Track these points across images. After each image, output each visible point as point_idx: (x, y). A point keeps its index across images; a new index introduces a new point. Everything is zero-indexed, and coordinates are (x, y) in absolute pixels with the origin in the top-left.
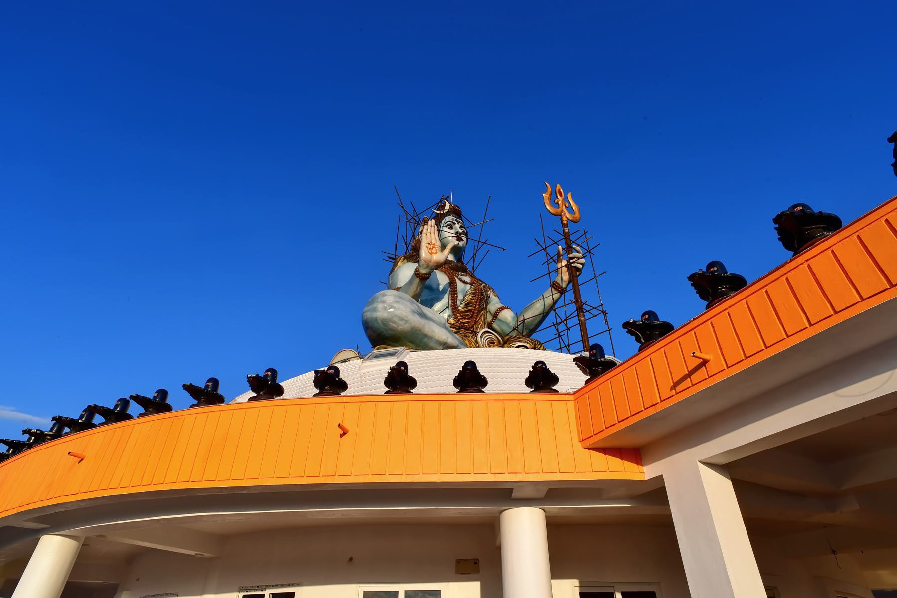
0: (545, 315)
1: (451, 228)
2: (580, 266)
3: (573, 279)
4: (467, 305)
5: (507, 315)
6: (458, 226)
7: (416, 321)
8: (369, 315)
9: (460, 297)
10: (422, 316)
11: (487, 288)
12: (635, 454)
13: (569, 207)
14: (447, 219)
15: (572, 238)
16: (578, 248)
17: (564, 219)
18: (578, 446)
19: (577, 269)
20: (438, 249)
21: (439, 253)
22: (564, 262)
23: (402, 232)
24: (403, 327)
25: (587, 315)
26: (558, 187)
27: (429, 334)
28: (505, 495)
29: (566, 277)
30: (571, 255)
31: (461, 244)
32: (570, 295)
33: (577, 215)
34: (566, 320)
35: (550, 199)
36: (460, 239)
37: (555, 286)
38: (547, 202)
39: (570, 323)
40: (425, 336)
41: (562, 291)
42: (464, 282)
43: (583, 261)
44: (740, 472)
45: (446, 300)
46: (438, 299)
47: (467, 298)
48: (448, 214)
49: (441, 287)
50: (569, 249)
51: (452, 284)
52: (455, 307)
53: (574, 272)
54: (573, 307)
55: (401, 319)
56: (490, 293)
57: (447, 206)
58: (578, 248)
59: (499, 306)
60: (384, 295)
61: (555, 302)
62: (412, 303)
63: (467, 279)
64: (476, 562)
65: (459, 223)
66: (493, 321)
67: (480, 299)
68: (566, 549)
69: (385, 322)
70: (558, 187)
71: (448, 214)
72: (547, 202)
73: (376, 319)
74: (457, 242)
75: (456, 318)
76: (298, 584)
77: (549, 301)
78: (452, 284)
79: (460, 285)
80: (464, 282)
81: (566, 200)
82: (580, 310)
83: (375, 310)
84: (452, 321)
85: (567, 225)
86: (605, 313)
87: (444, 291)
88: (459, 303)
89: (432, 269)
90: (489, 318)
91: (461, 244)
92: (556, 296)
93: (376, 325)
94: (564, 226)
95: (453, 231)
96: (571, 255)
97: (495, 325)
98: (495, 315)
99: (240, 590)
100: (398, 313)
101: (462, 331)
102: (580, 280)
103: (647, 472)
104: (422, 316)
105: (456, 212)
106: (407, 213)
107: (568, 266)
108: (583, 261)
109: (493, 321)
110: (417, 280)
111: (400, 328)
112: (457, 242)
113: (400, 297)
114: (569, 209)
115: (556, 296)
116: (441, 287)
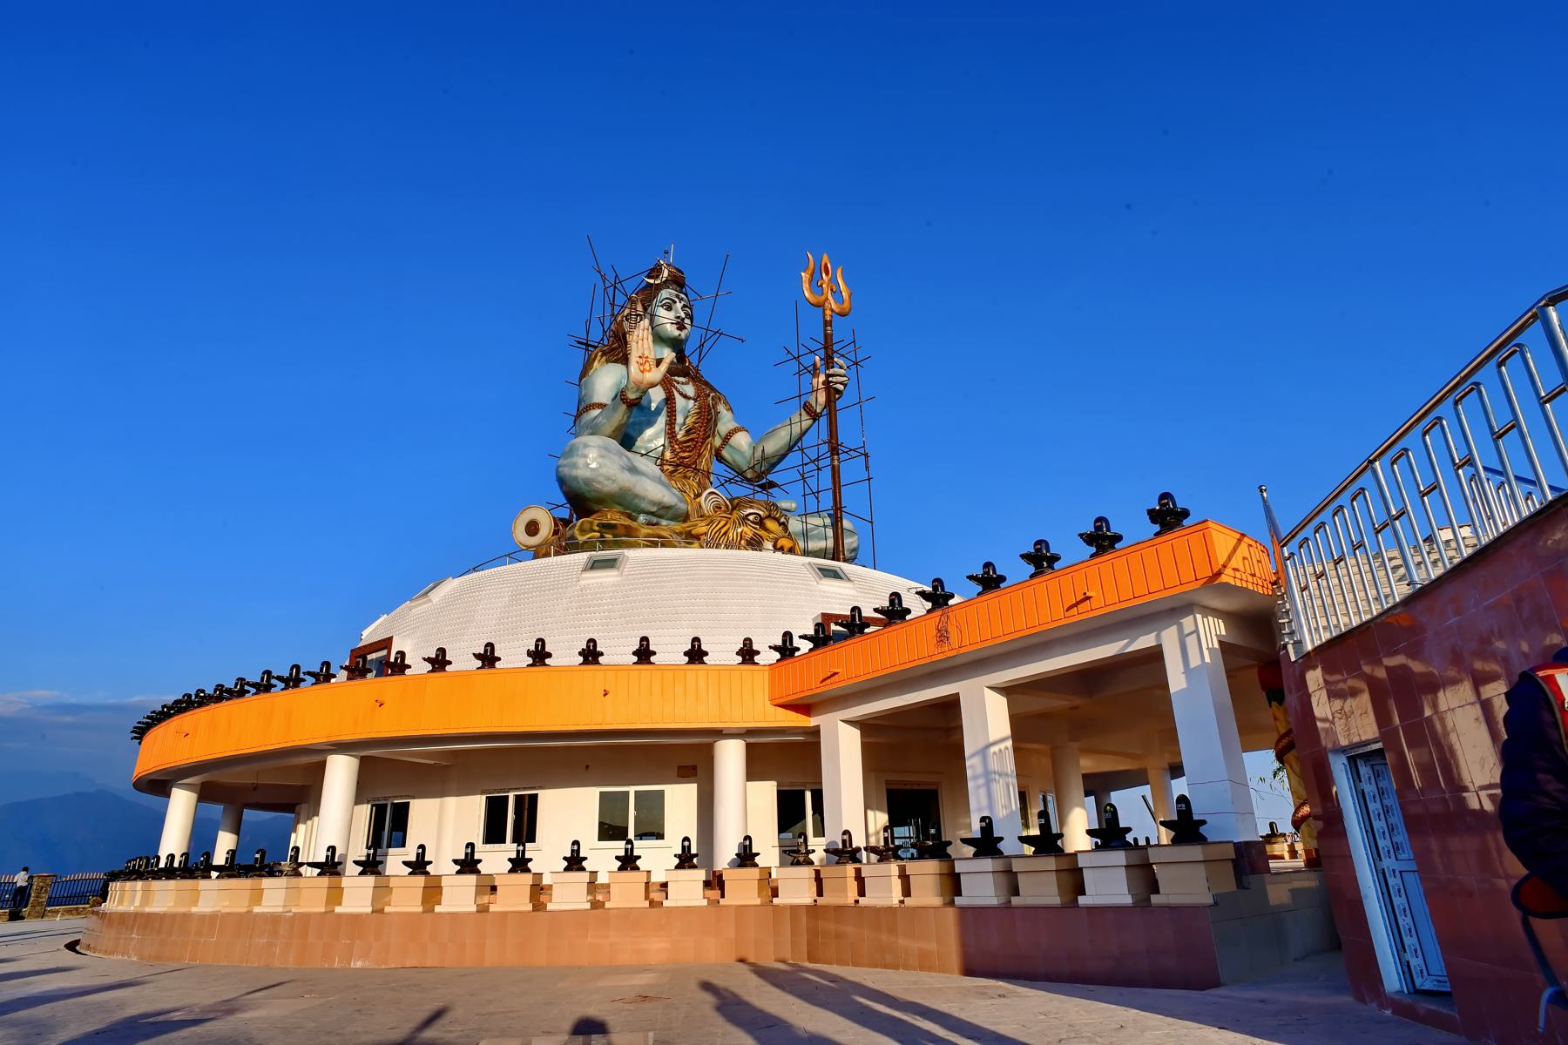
0: (790, 448)
1: (669, 308)
2: (841, 387)
3: (830, 403)
4: (688, 432)
5: (742, 440)
6: (679, 305)
7: (625, 479)
8: (565, 471)
9: (679, 419)
10: (633, 470)
11: (717, 399)
12: (805, 708)
13: (839, 290)
14: (664, 293)
15: (835, 348)
16: (841, 362)
17: (828, 312)
18: (768, 703)
19: (838, 391)
20: (653, 363)
21: (654, 369)
22: (822, 378)
23: (598, 313)
24: (609, 487)
25: (843, 457)
26: (825, 259)
27: (642, 493)
28: (720, 734)
29: (822, 397)
30: (831, 371)
31: (683, 334)
32: (824, 421)
33: (846, 305)
34: (818, 459)
35: (810, 282)
36: (681, 327)
37: (808, 408)
38: (806, 286)
39: (821, 464)
40: (637, 496)
41: (815, 417)
42: (685, 397)
44: (866, 726)
45: (661, 421)
46: (650, 424)
47: (689, 421)
48: (665, 284)
49: (653, 406)
50: (829, 361)
51: (669, 401)
52: (671, 434)
53: (832, 393)
54: (825, 448)
55: (608, 479)
56: (721, 407)
57: (666, 273)
58: (841, 362)
59: (733, 425)
60: (586, 446)
61: (803, 433)
62: (620, 455)
63: (690, 390)
64: (694, 768)
66: (722, 446)
67: (707, 418)
68: (754, 770)
69: (587, 482)
70: (825, 259)
71: (665, 284)
72: (806, 286)
73: (576, 478)
74: (677, 333)
75: (673, 451)
76: (541, 788)
77: (796, 430)
78: (669, 401)
79: (680, 402)
80: (685, 397)
81: (834, 280)
82: (834, 450)
83: (574, 466)
84: (668, 455)
85: (827, 323)
86: (866, 455)
87: (658, 412)
89: (645, 392)
90: (718, 442)
91: (683, 334)
92: (806, 424)
93: (574, 484)
94: (827, 323)
95: (671, 315)
96: (831, 371)
97: (725, 453)
98: (726, 439)
99: (483, 793)
100: (603, 471)
101: (681, 469)
102: (840, 404)
103: (812, 722)
105: (677, 282)
106: (604, 279)
107: (827, 383)
109: (722, 446)
110: (624, 407)
111: (606, 489)
112: (677, 333)
113: (606, 449)
114: (836, 293)
115: (807, 423)
116: (653, 406)
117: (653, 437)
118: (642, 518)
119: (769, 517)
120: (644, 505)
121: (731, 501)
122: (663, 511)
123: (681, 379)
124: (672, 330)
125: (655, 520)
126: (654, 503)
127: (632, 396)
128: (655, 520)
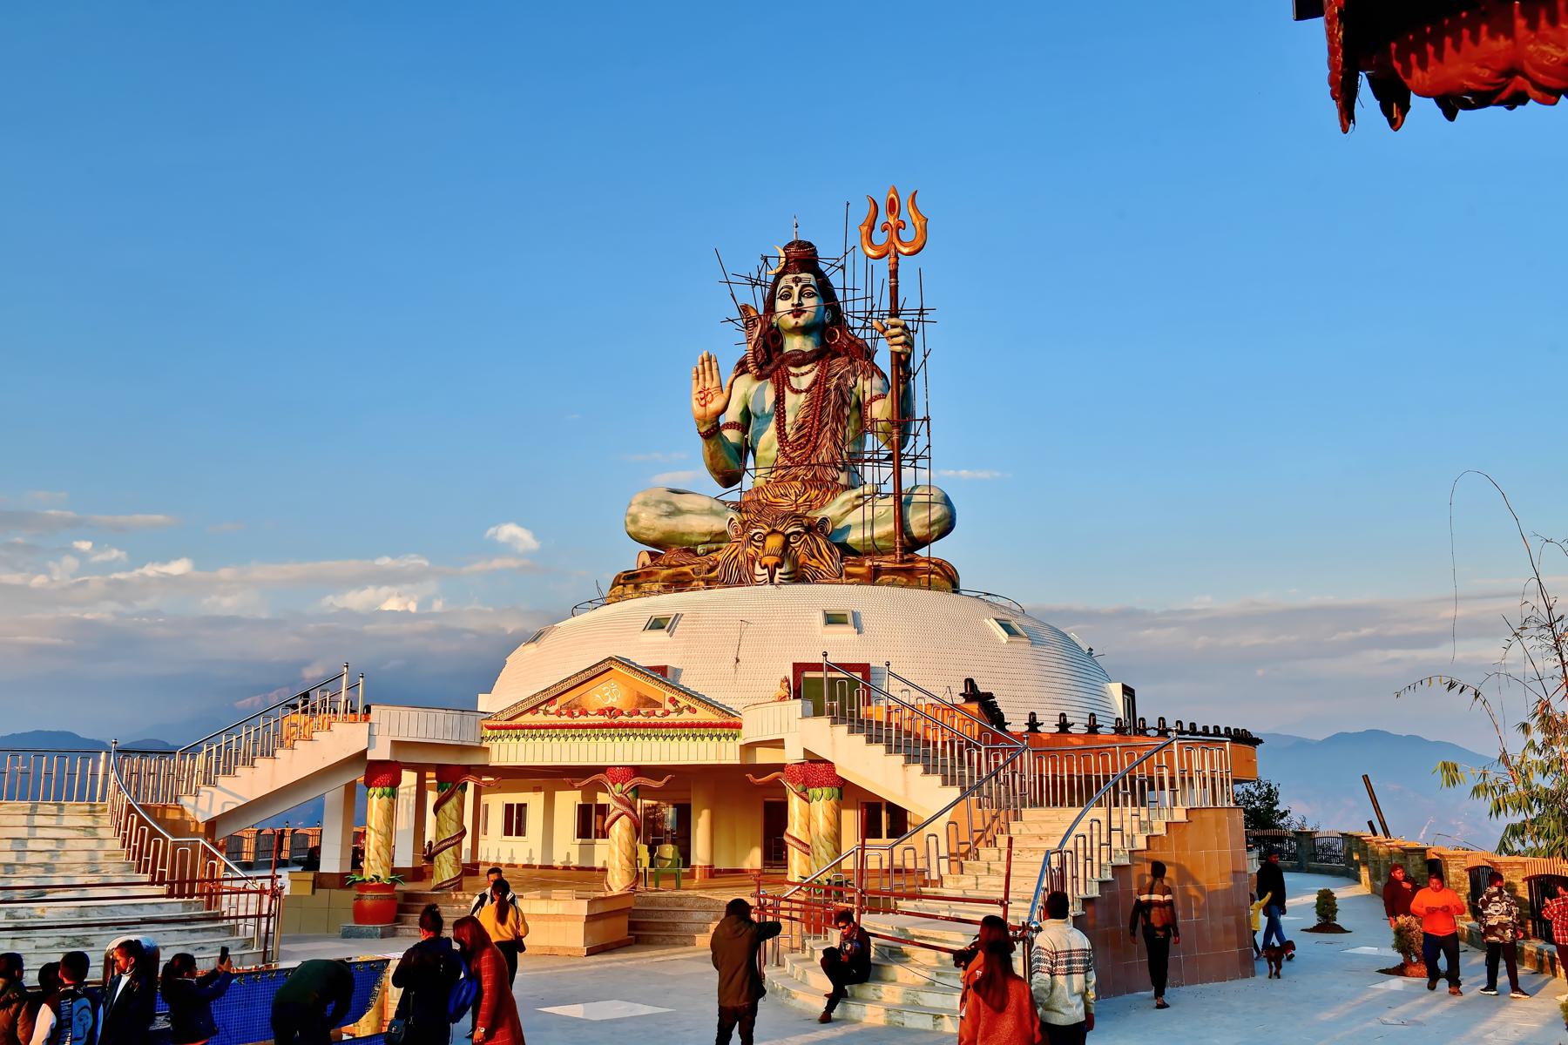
1: (787, 296)
2: (899, 348)
4: (798, 430)
6: (796, 290)
9: (790, 418)
14: (782, 283)
27: (687, 530)
36: (798, 311)
43: (902, 338)
51: (780, 400)
65: (797, 281)
78: (780, 400)
86: (927, 419)
87: (769, 416)
88: (788, 429)
91: (801, 321)
104: (676, 512)
108: (902, 338)
117: (767, 442)
118: (700, 549)
119: (774, 532)
120: (695, 539)
121: (743, 523)
122: (719, 538)
123: (805, 369)
124: (791, 321)
125: (714, 546)
126: (705, 535)
127: (703, 430)
128: (714, 546)
